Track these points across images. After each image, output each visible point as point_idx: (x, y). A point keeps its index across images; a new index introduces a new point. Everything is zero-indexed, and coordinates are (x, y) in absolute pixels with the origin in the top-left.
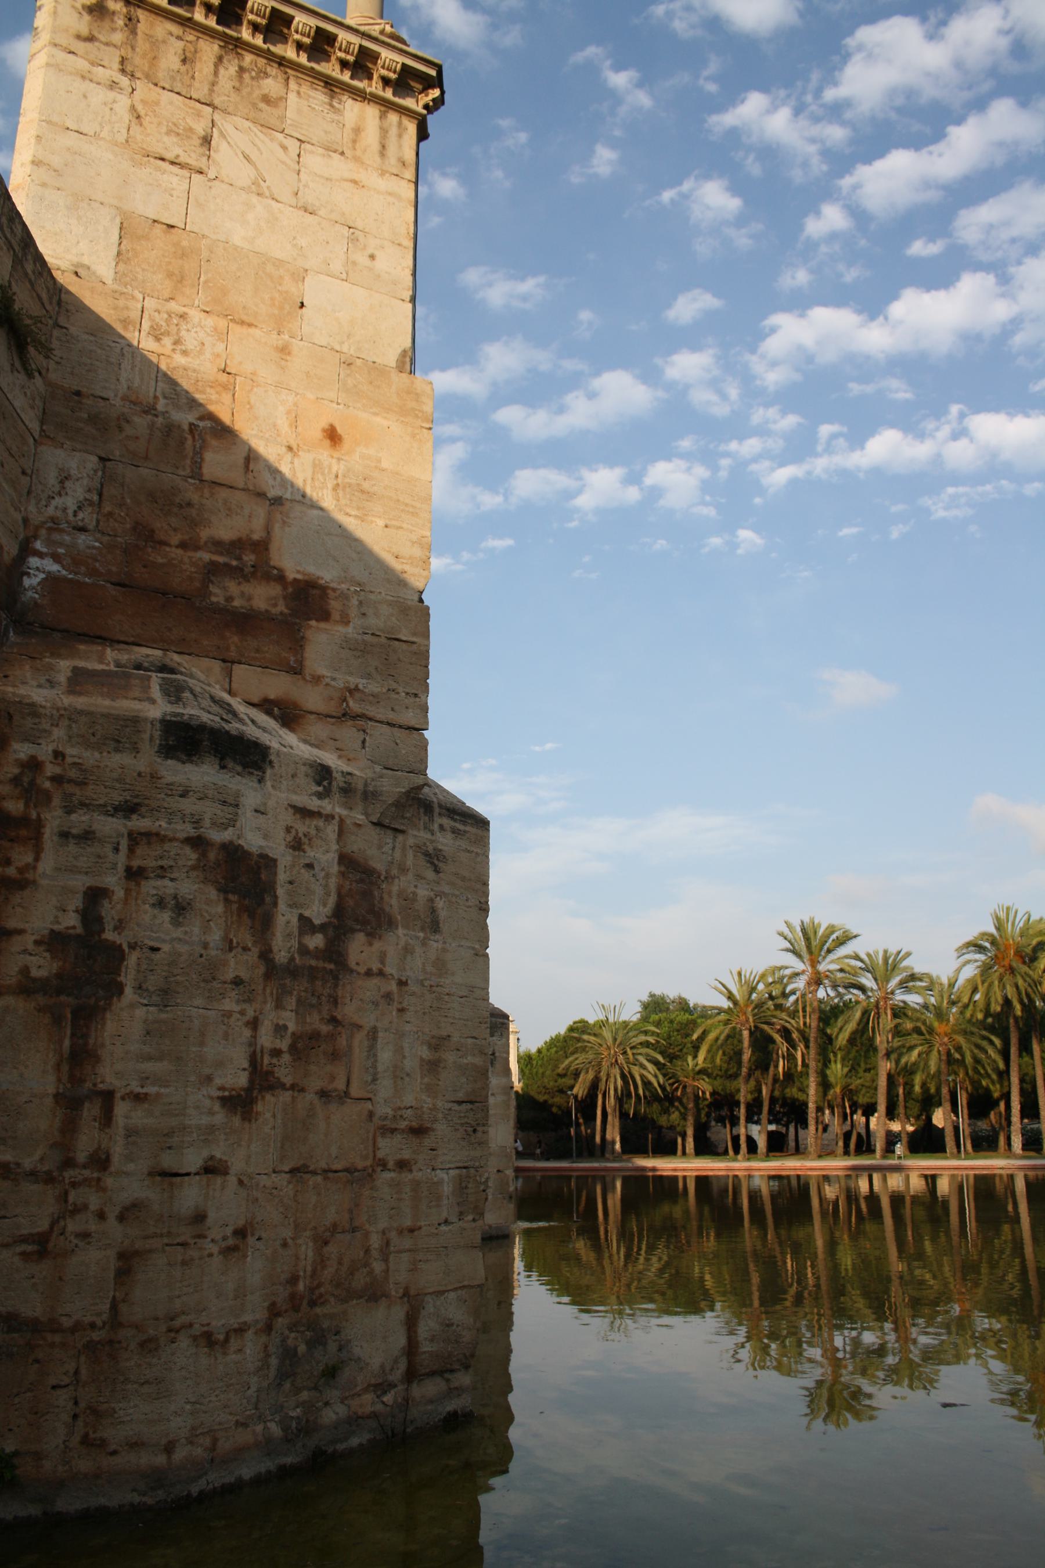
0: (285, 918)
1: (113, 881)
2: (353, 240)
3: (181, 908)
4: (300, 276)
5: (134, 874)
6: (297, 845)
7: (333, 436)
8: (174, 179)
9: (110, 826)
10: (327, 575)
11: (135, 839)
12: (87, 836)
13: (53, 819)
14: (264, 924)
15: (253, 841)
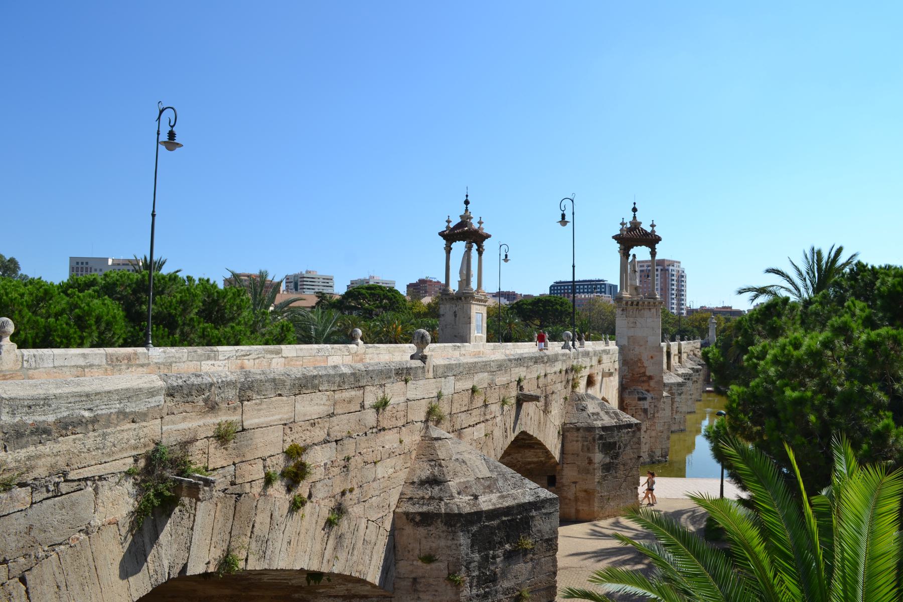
0: (649, 413)
1: (634, 413)
2: (653, 330)
3: (640, 415)
4: (647, 337)
5: (636, 412)
6: (650, 406)
7: (652, 357)
8: (633, 329)
9: (633, 408)
10: (651, 374)
11: (636, 409)
12: (632, 409)
13: (629, 408)
14: (647, 415)
15: (646, 407)
